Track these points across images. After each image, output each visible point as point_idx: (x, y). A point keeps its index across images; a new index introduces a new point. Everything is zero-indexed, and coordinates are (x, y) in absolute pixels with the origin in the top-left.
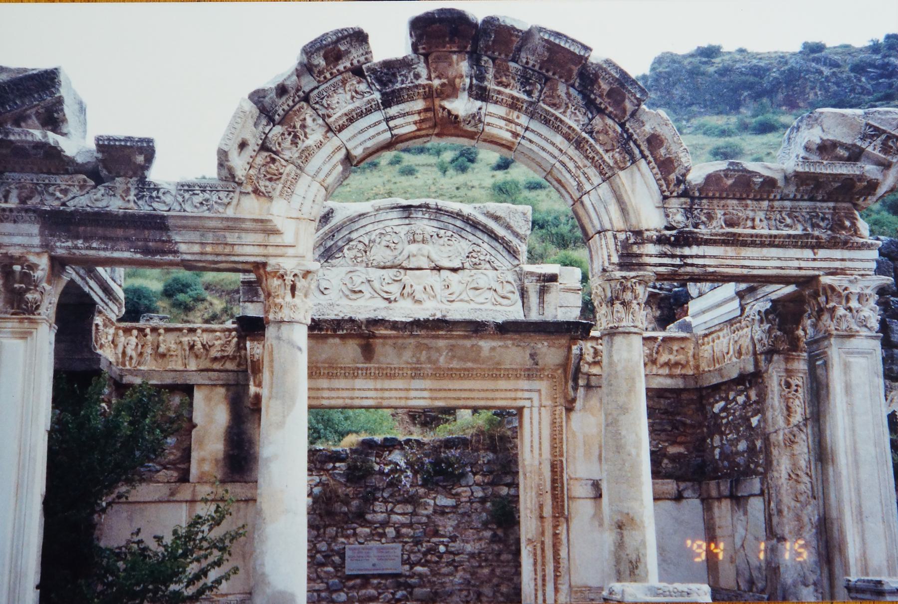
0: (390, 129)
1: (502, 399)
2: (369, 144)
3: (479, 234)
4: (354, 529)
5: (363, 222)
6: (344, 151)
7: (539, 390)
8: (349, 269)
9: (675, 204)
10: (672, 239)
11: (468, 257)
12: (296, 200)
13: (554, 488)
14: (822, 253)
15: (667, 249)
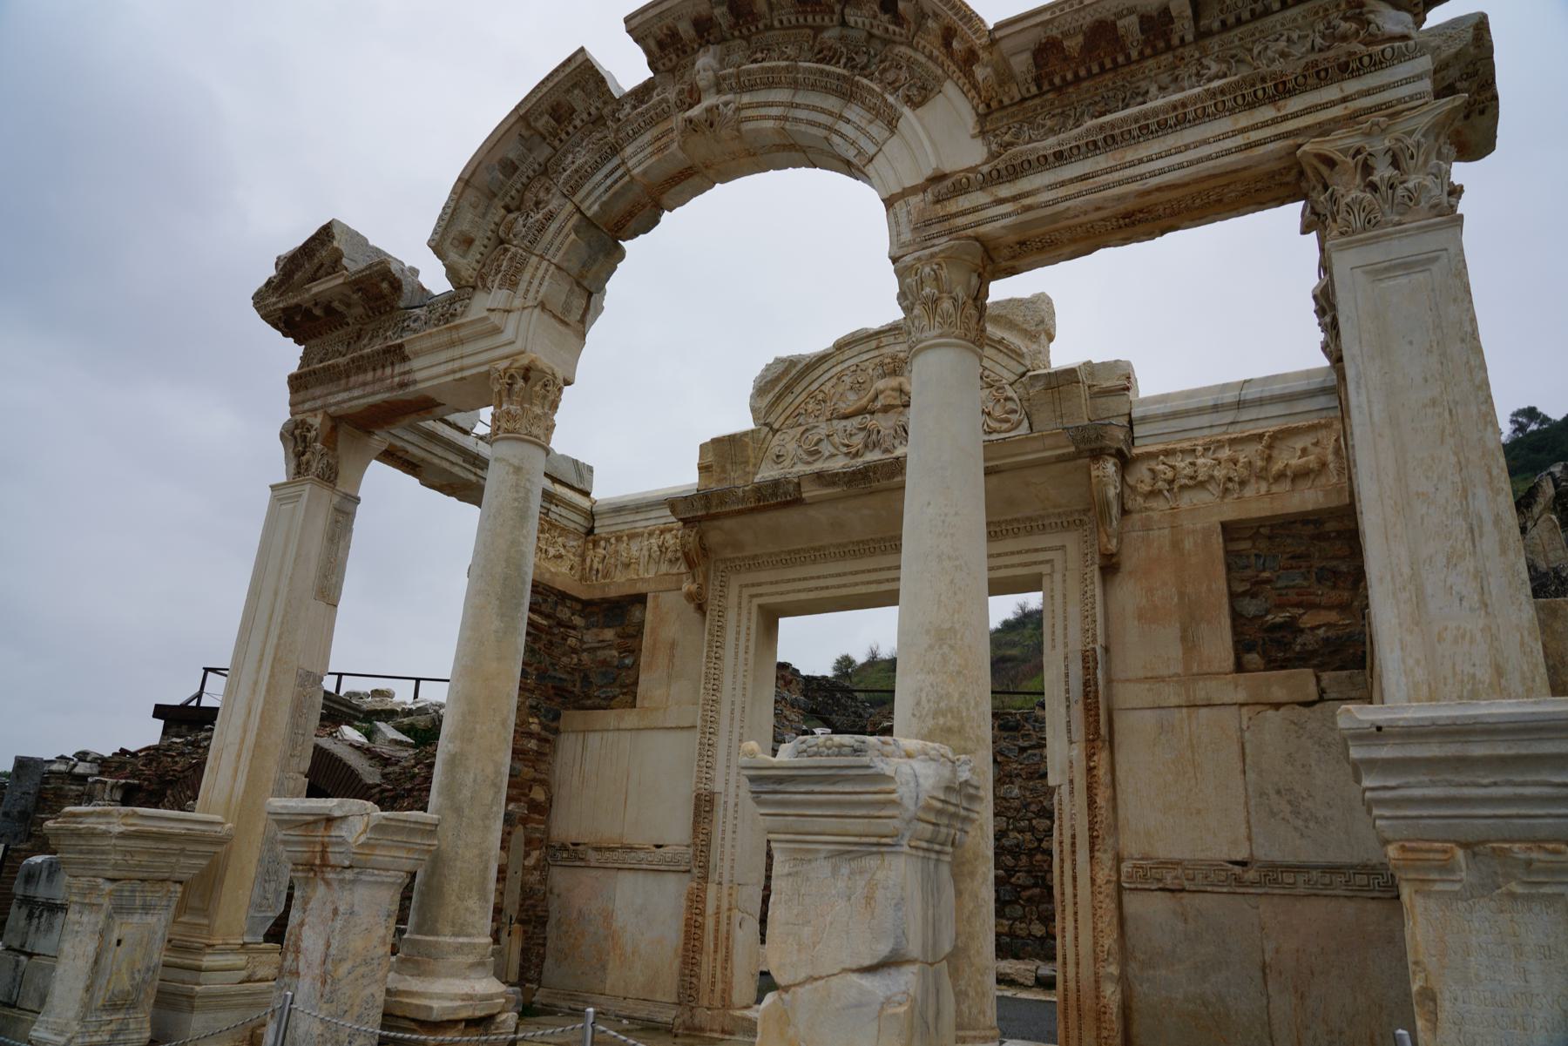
0: (629, 170)
1: (1006, 567)
2: (604, 198)
4: (1030, 820)
5: (825, 366)
6: (577, 216)
7: (1063, 547)
8: (802, 429)
12: (523, 286)
13: (1086, 695)
14: (1294, 104)
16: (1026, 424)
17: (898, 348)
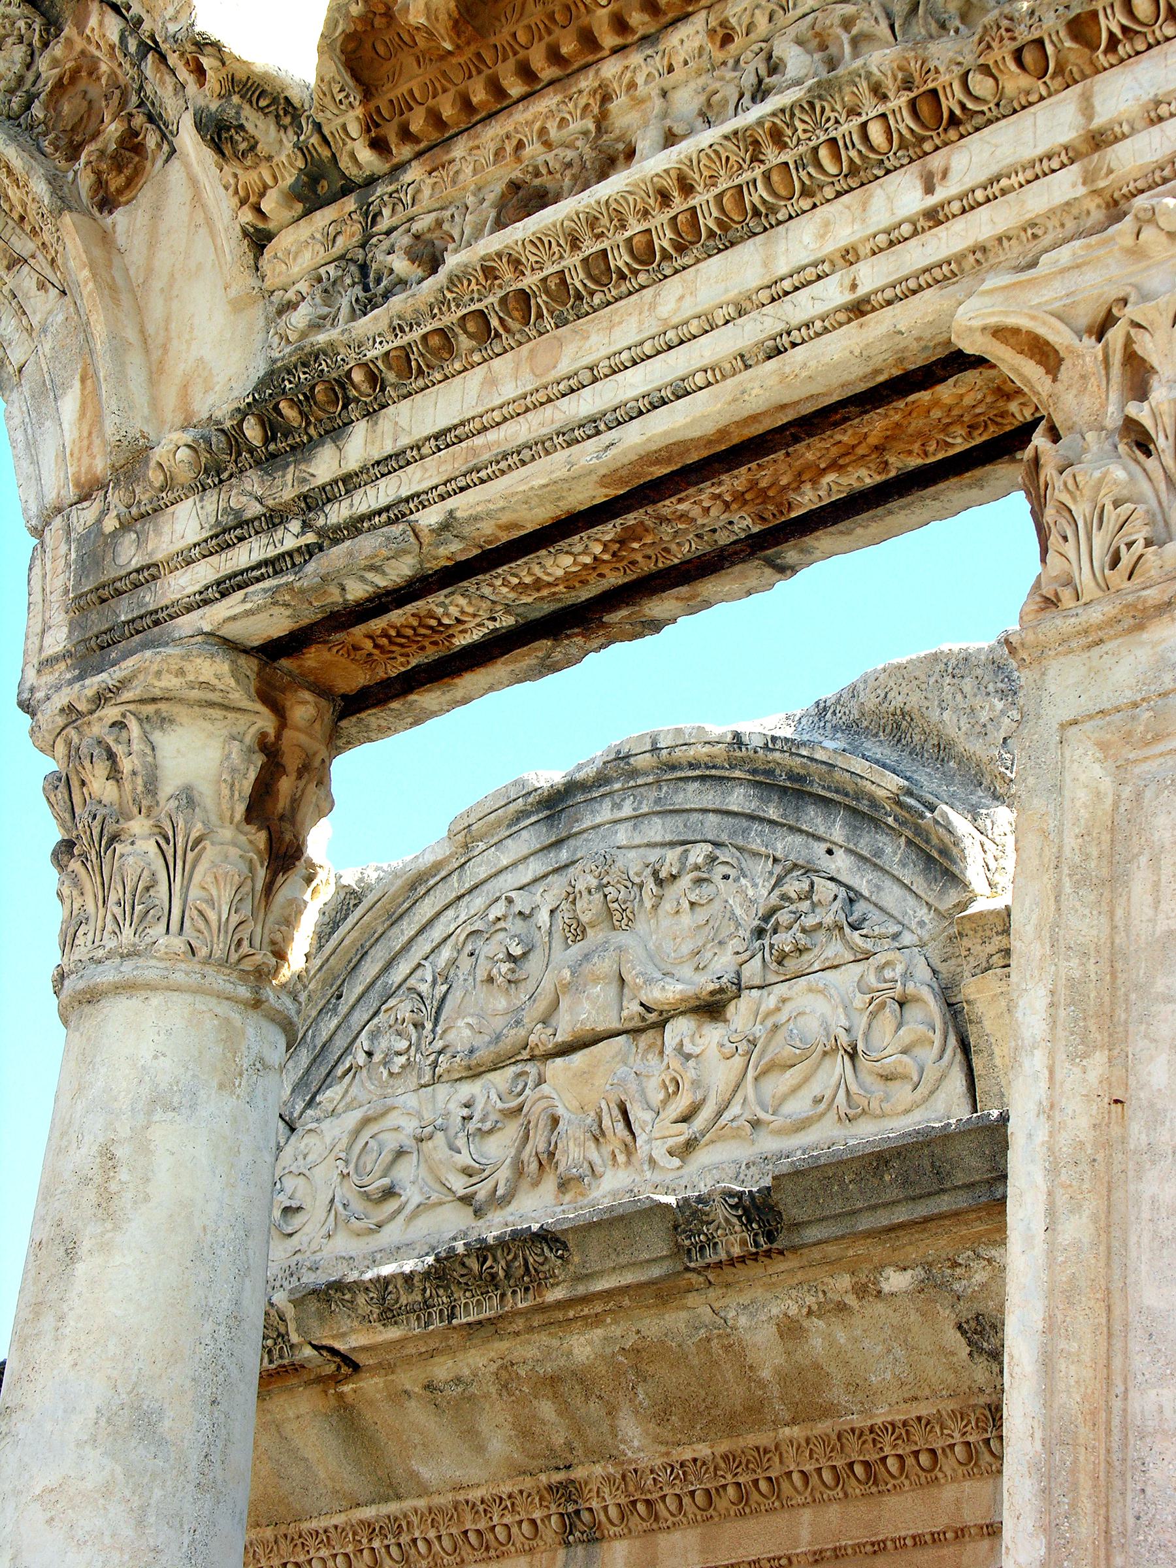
3: (813, 818)
5: (426, 909)
9: (305, 246)
10: (252, 432)
11: (760, 933)
14: (969, 161)
15: (250, 492)
16: (957, 1082)
17: (622, 835)
